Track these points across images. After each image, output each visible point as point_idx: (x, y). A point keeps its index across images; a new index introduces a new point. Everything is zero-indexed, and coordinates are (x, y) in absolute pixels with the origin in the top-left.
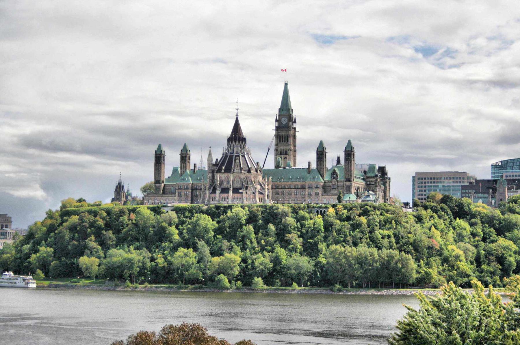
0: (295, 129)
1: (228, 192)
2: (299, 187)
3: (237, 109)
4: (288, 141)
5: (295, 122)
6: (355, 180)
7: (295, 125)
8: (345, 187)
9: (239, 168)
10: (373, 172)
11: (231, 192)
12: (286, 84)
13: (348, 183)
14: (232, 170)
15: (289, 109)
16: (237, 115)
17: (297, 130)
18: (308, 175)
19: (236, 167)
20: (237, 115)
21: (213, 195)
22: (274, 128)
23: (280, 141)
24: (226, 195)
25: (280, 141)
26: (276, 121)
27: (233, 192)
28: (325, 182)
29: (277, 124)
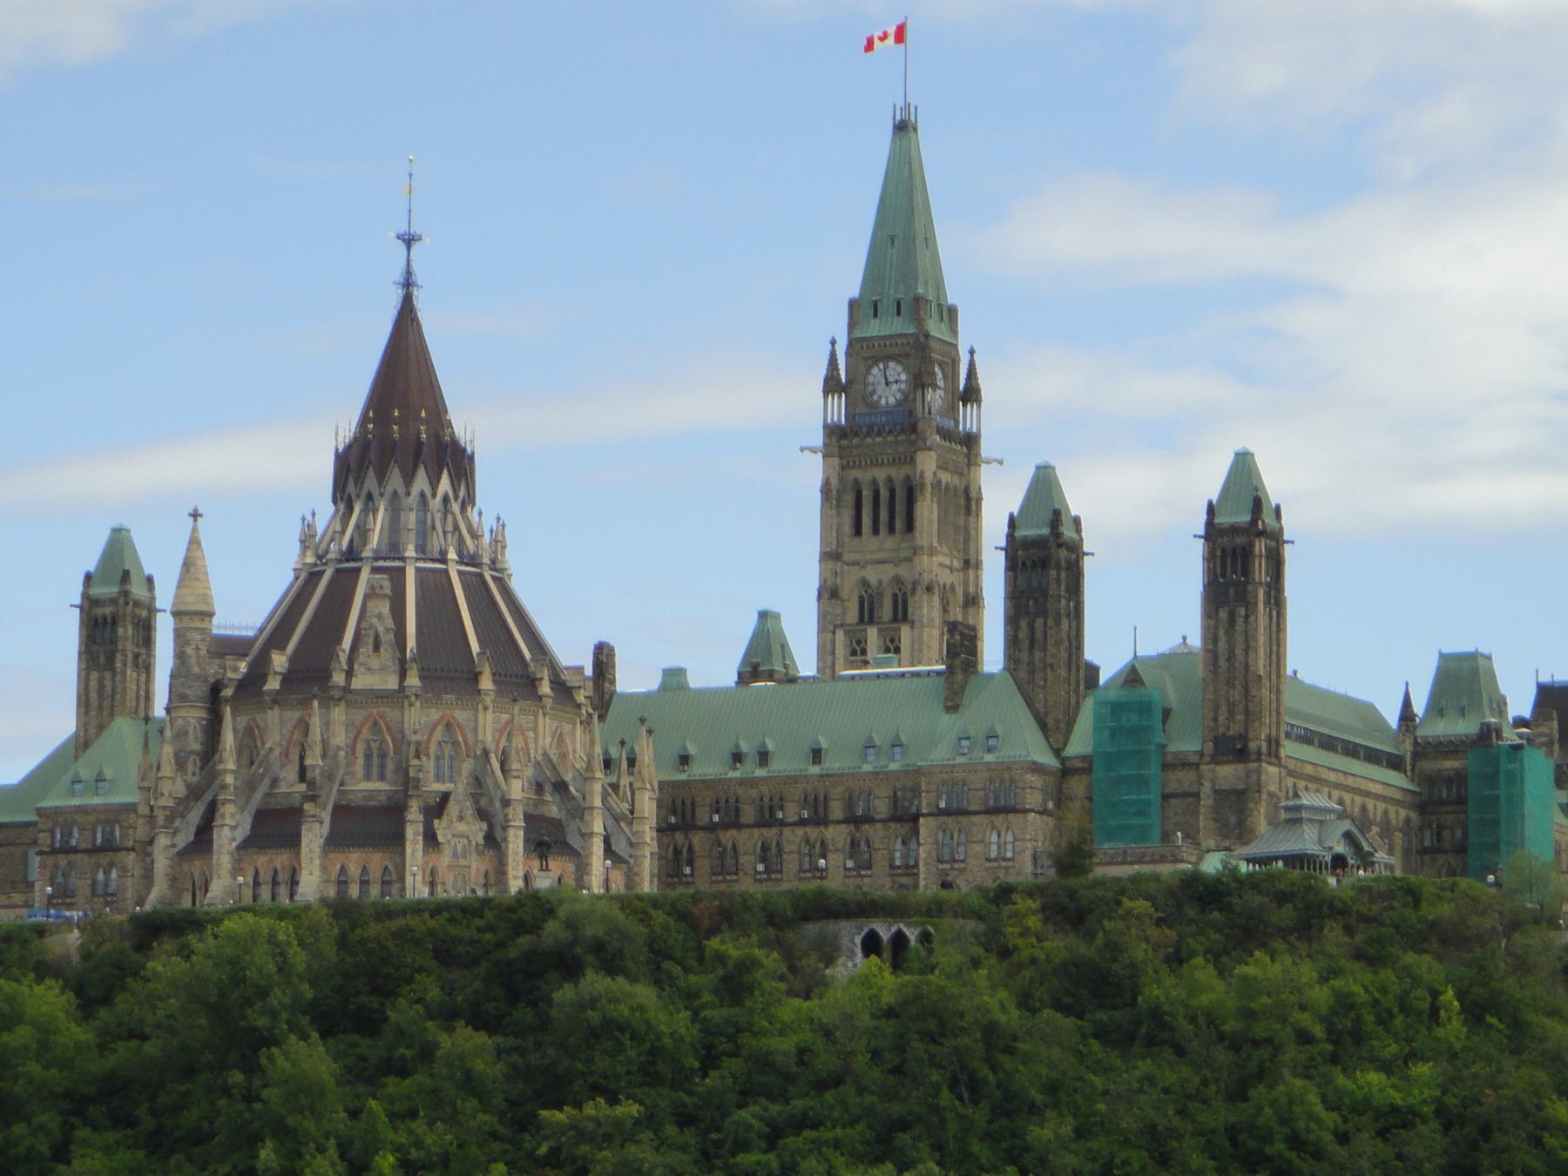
0: (971, 441)
1: (292, 842)
2: (882, 807)
3: (409, 240)
4: (910, 526)
5: (971, 394)
6: (1289, 749)
7: (968, 418)
8: (1207, 801)
9: (387, 653)
10: (1462, 712)
11: (313, 837)
12: (903, 127)
13: (1228, 774)
14: (338, 678)
15: (918, 301)
16: (408, 284)
17: (986, 448)
18: (947, 719)
19: (366, 649)
20: (408, 284)
21: (197, 867)
22: (818, 439)
23: (858, 531)
24: (281, 859)
25: (858, 531)
26: (832, 385)
27: (336, 841)
28: (1066, 772)
29: (837, 409)
